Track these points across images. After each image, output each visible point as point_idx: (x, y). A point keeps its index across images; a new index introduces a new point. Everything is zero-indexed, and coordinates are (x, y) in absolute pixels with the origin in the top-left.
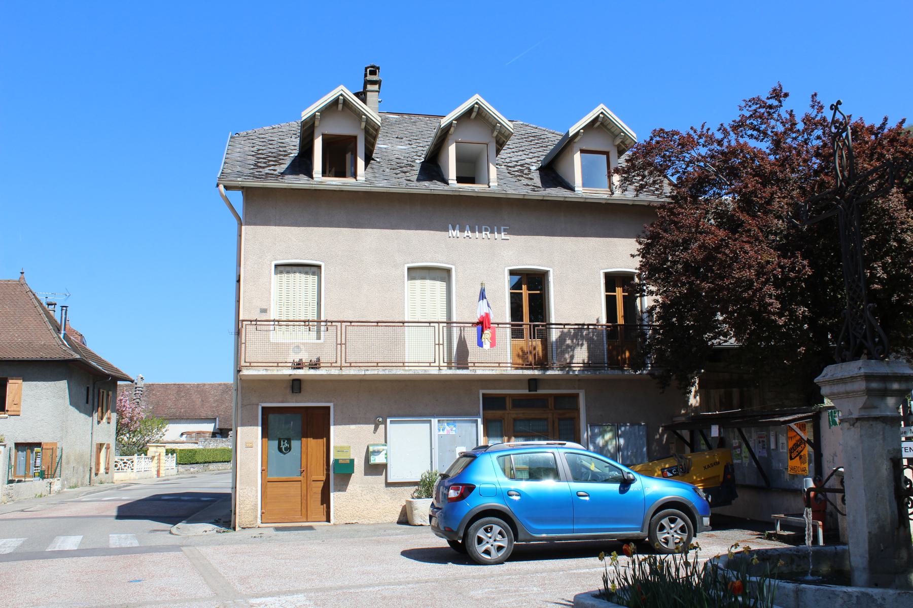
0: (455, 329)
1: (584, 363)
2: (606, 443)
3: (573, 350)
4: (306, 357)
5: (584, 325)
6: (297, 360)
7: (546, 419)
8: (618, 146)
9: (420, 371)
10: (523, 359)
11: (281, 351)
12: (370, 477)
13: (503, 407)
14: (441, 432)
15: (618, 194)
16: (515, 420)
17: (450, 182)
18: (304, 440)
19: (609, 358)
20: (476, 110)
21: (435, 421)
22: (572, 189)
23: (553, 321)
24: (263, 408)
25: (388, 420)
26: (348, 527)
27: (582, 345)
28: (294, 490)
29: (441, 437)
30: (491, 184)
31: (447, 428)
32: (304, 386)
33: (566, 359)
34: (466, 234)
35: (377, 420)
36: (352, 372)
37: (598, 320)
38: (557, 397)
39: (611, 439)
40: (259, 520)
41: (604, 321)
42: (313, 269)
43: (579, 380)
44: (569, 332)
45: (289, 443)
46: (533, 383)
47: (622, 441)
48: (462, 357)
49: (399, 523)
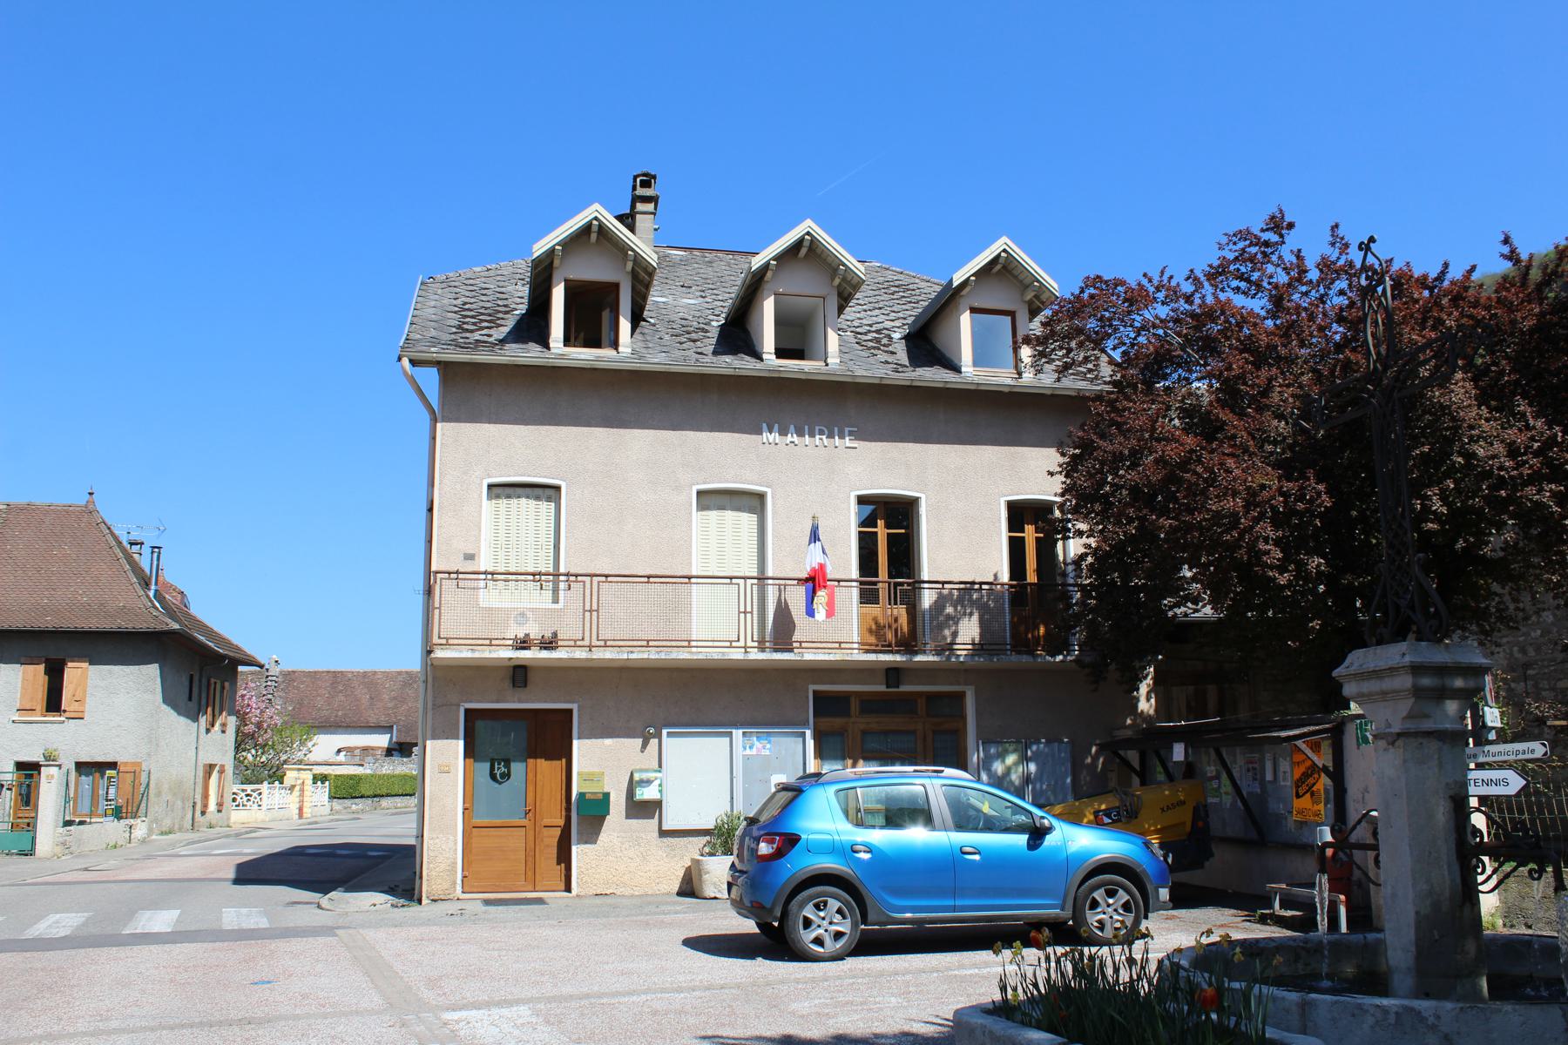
2: (1008, 771)
3: (957, 624)
4: (535, 631)
5: (973, 583)
6: (521, 635)
7: (914, 732)
8: (1030, 303)
9: (715, 654)
10: (877, 635)
11: (494, 620)
12: (634, 822)
13: (845, 712)
14: (748, 752)
15: (1028, 377)
16: (864, 733)
18: (531, 761)
19: (1013, 636)
20: (806, 244)
21: (737, 733)
22: (957, 370)
23: (925, 576)
24: (467, 711)
25: (664, 732)
26: (598, 900)
27: (971, 614)
28: (516, 840)
29: (747, 758)
31: (757, 744)
32: (531, 675)
33: (945, 638)
34: (789, 438)
35: (646, 730)
36: (608, 654)
38: (931, 697)
39: (1016, 764)
40: (459, 888)
41: (1005, 577)
42: (549, 492)
44: (951, 594)
45: (508, 766)
46: (893, 674)
47: (1032, 767)
48: (782, 631)
49: (680, 894)
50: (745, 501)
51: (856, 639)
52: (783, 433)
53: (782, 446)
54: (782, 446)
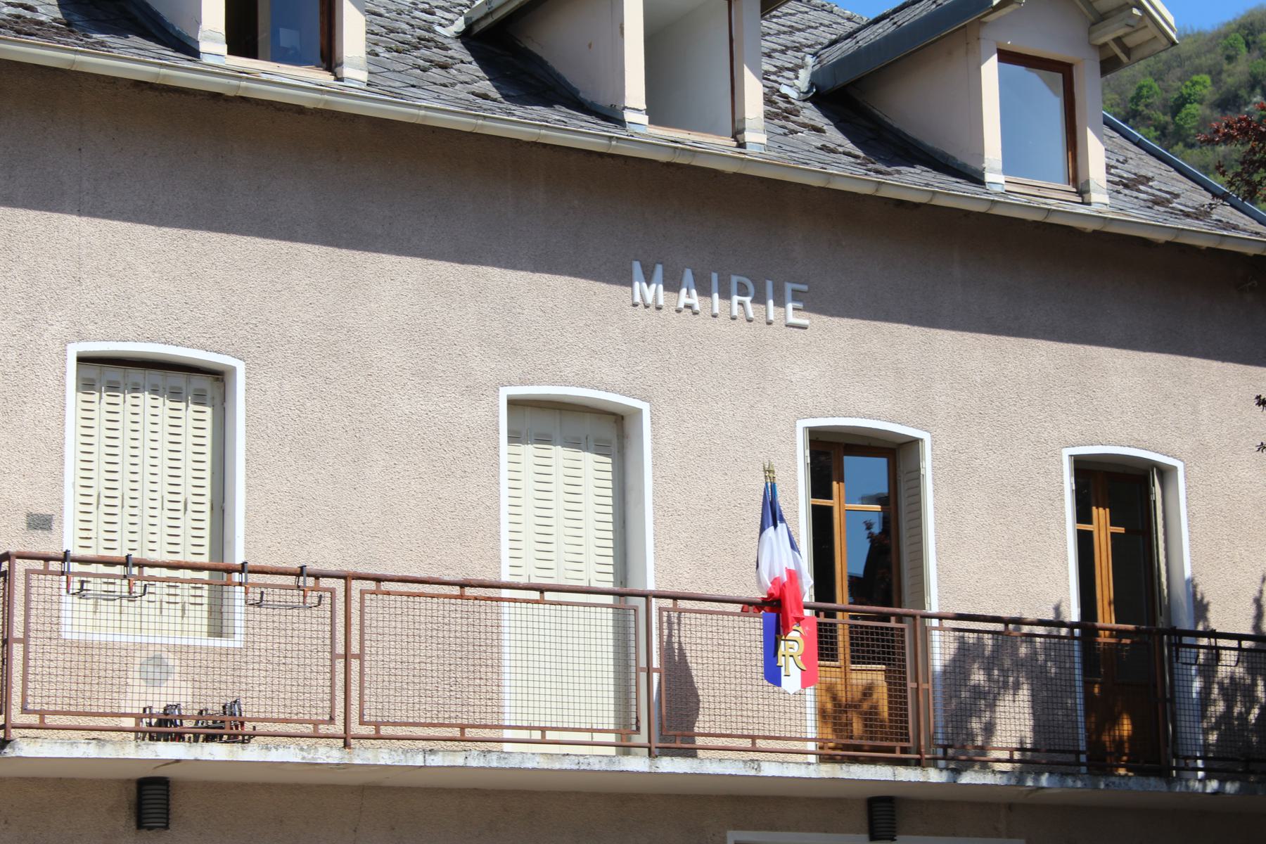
0: (936, 637)
1: (1022, 750)
3: (992, 706)
4: (177, 692)
5: (1019, 621)
6: (158, 709)
10: (849, 727)
17: (629, 116)
19: (1089, 743)
22: (976, 178)
23: (934, 604)
27: (1017, 687)
30: (749, 137)
32: (179, 804)
33: (971, 736)
34: (683, 298)
37: (1057, 609)
41: (1073, 613)
42: (202, 382)
43: (1010, 807)
48: (674, 712)
50: (587, 426)
51: (811, 732)
52: (672, 285)
53: (668, 312)
54: (668, 312)
